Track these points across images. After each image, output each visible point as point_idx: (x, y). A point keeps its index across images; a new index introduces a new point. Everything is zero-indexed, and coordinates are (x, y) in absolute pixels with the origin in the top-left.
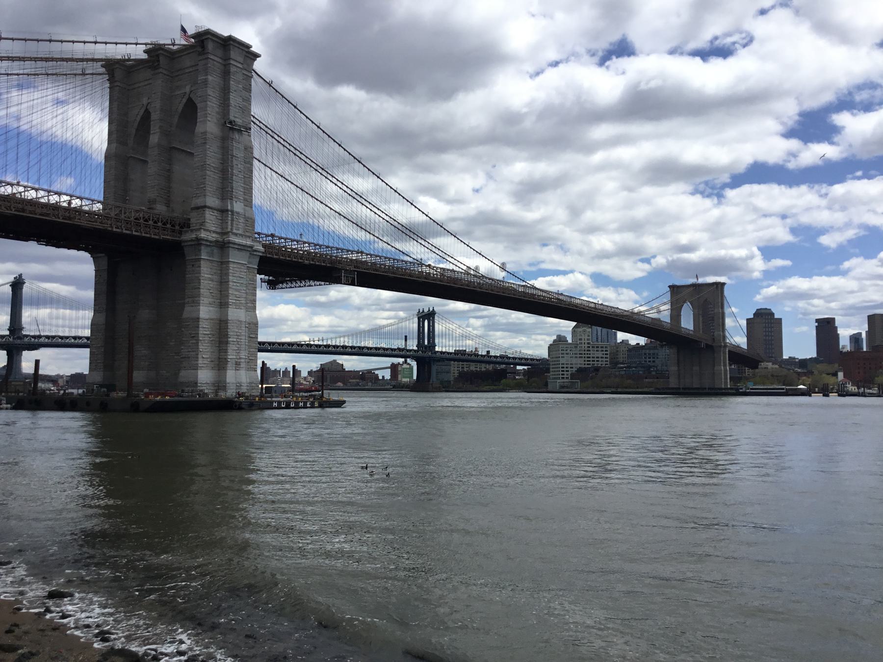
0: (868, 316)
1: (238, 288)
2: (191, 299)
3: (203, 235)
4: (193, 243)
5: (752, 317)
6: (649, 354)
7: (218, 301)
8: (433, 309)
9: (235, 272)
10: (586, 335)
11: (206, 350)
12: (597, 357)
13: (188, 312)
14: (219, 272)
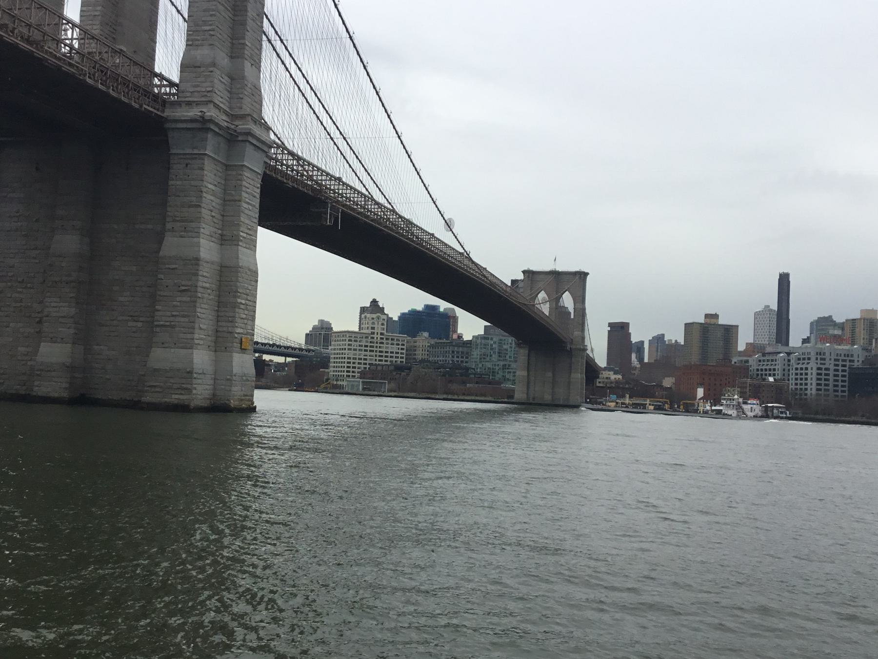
0: (686, 324)
1: (249, 213)
2: (179, 224)
3: (211, 112)
4: (189, 126)
6: (458, 352)
7: (220, 232)
9: (247, 185)
10: (380, 323)
11: (203, 316)
12: (392, 353)
13: (171, 246)
14: (223, 182)
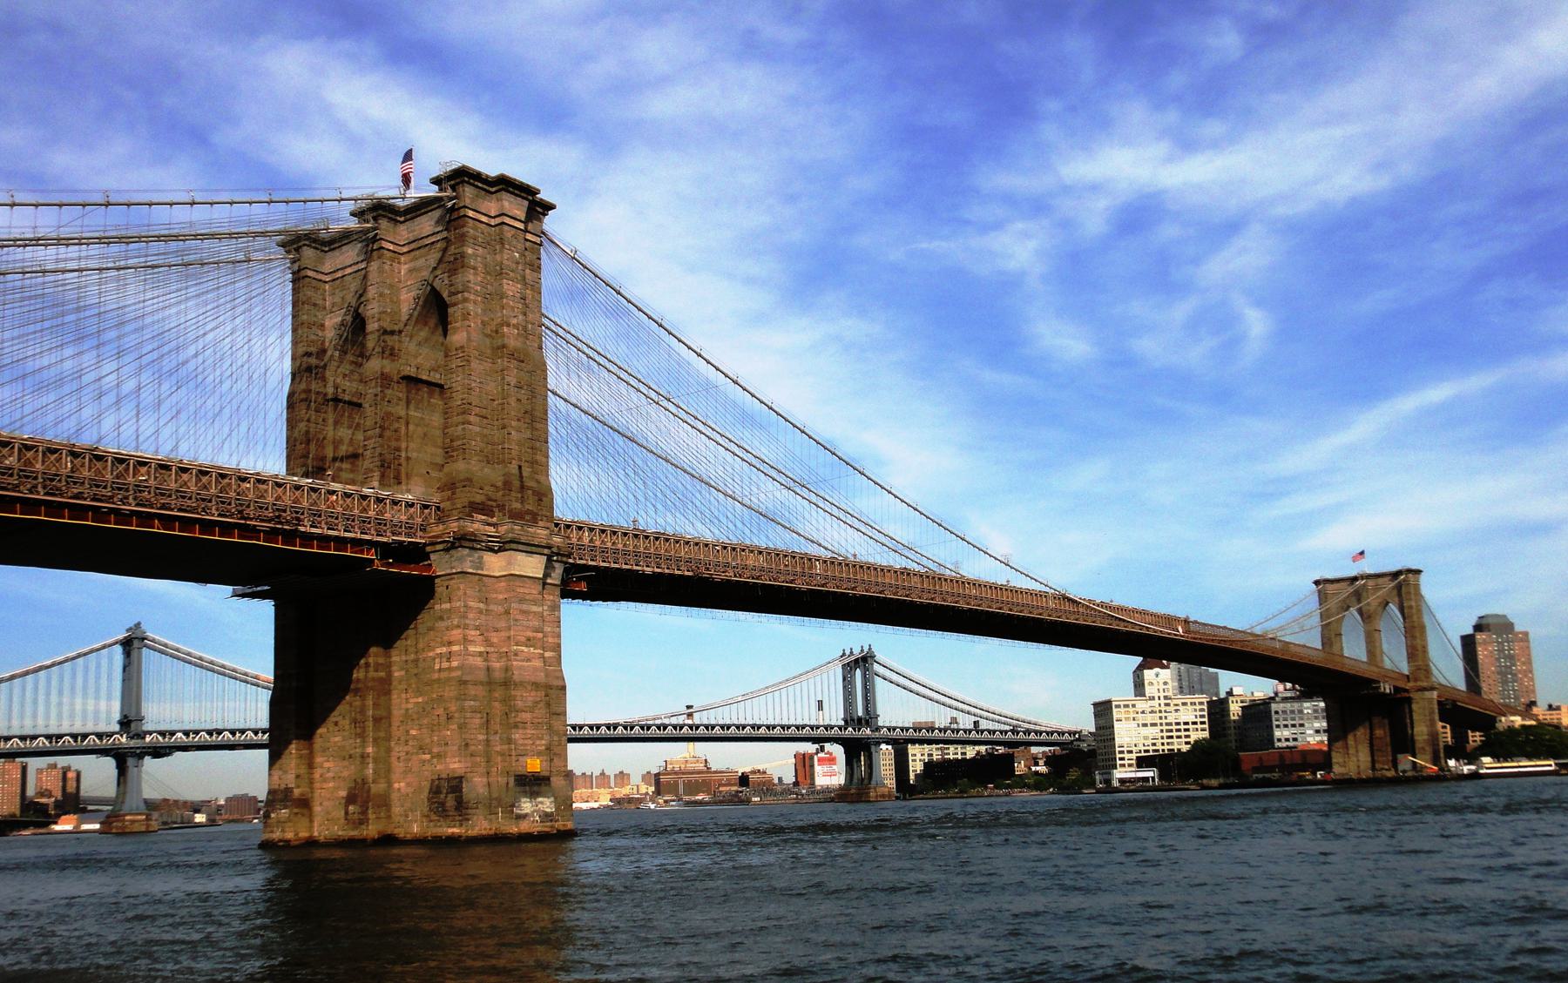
2: (444, 650)
5: (1470, 631)
8: (870, 649)
